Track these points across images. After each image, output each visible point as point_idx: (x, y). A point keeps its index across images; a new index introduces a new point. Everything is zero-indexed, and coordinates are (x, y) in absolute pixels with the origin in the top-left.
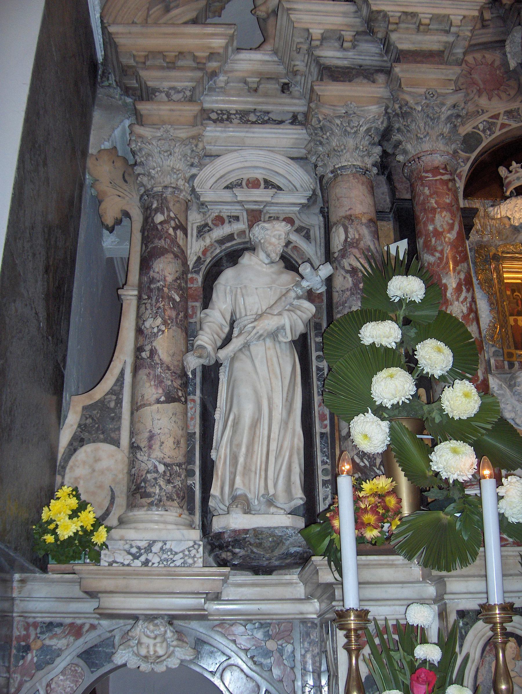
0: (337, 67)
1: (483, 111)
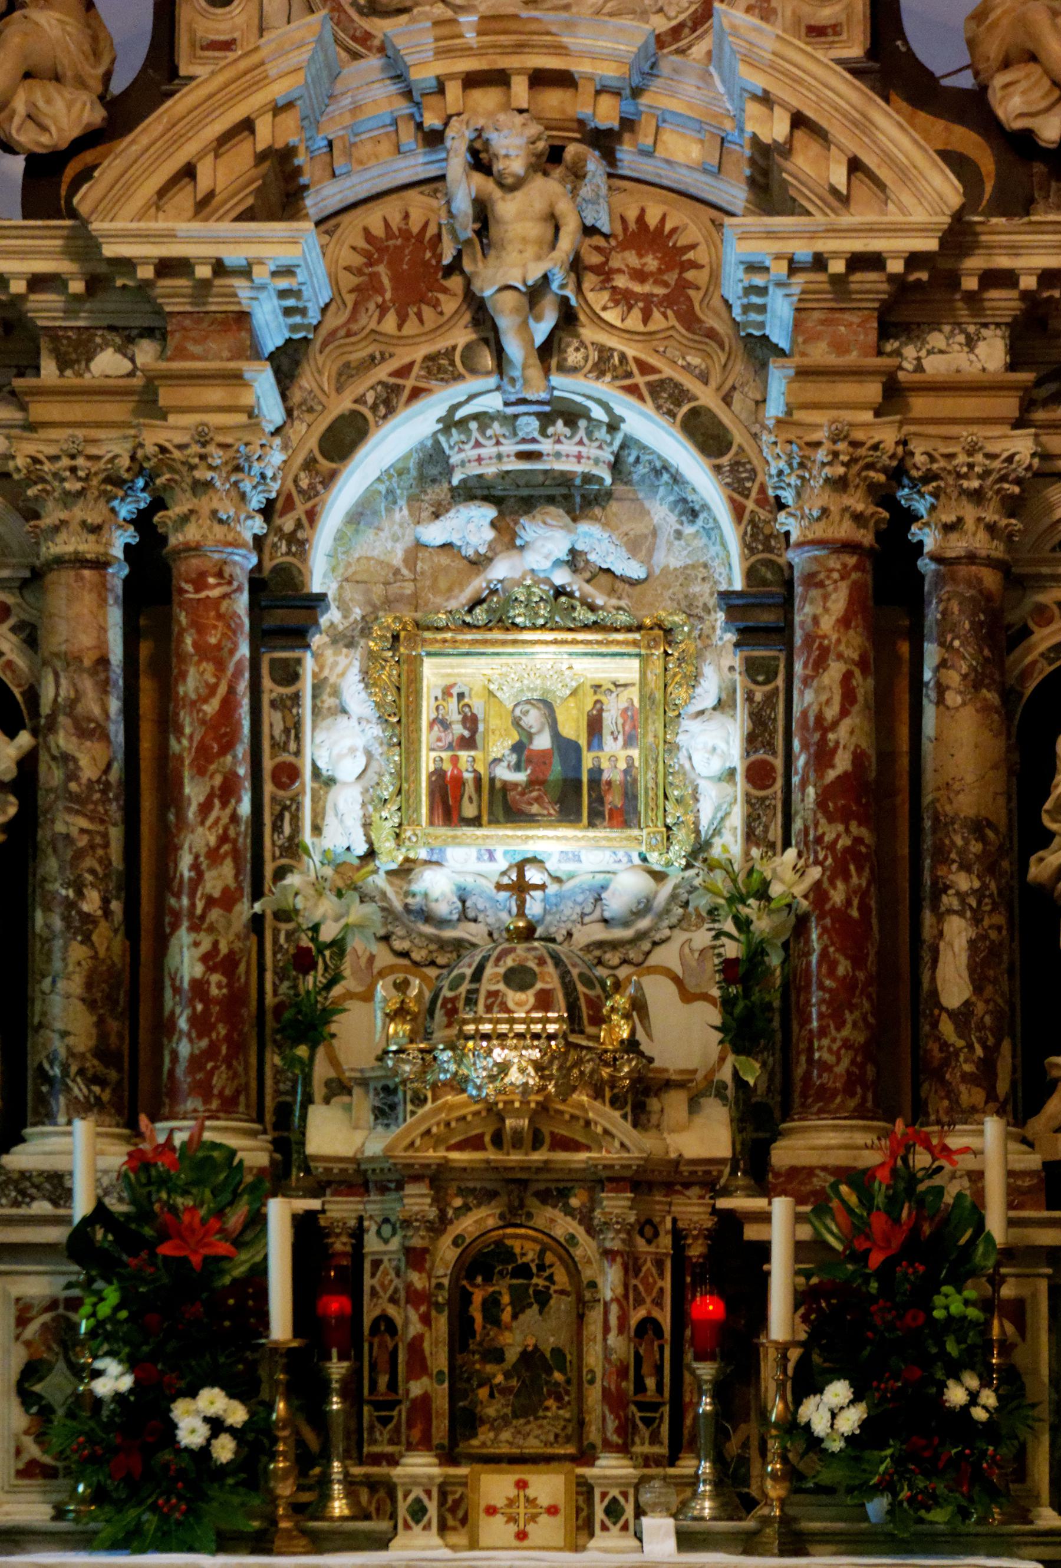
1: (382, 354)
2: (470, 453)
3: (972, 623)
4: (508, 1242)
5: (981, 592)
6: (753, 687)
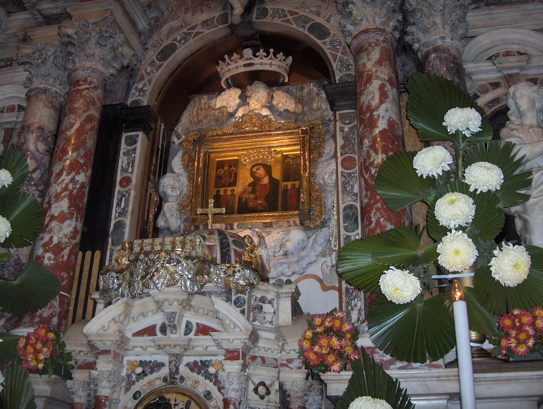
0: (53, 15)
1: (186, 25)
2: (226, 69)
3: (447, 68)
4: (167, 396)
5: (450, 55)
6: (343, 126)
